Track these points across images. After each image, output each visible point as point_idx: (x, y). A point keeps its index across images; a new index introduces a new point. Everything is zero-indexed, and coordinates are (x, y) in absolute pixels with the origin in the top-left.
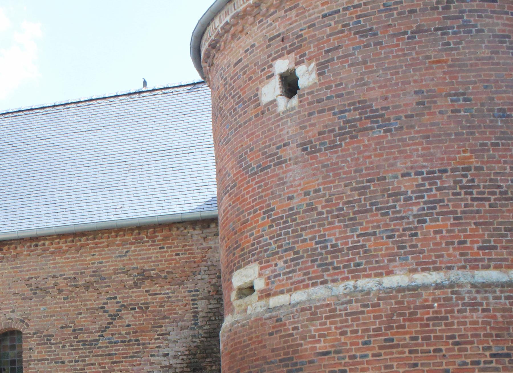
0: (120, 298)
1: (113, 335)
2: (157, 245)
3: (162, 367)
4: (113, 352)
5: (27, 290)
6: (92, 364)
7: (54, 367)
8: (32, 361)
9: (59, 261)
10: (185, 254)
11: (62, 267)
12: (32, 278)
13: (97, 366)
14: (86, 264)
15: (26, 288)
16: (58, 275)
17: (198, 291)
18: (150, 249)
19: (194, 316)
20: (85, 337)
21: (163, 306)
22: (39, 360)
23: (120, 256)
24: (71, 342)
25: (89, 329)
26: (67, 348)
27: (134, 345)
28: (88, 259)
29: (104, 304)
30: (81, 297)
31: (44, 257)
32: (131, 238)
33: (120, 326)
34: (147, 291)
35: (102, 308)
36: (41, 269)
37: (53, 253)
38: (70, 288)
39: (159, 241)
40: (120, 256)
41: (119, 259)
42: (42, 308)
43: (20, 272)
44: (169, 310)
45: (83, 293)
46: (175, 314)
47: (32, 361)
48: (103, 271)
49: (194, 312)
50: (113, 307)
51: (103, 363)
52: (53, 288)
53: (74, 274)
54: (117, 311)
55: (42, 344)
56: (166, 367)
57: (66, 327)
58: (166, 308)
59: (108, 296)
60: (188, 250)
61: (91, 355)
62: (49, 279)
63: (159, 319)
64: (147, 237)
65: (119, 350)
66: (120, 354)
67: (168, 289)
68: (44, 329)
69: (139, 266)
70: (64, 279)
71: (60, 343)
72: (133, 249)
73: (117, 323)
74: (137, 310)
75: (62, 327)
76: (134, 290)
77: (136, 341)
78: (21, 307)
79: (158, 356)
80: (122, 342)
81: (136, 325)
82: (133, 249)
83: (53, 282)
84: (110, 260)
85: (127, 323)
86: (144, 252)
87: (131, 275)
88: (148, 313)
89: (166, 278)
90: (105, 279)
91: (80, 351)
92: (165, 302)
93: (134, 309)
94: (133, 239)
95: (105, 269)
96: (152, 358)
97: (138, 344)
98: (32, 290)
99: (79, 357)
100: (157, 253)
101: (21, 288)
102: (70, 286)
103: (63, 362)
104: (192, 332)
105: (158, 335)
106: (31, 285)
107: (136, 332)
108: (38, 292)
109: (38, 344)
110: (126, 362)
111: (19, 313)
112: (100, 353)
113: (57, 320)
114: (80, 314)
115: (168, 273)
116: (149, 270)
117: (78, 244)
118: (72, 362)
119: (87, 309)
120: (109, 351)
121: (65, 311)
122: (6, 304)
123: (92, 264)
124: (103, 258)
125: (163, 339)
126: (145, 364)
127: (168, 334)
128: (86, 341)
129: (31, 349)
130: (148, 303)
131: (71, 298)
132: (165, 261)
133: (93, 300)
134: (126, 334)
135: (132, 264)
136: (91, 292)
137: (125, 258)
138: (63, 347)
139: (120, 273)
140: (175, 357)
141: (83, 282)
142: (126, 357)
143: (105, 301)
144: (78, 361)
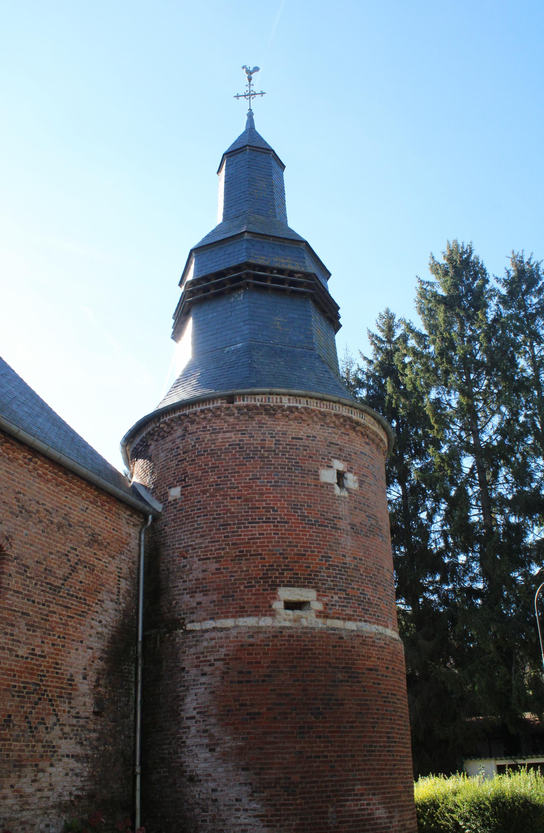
16: (41, 502)
20: (51, 580)
21: (102, 573)
52: (35, 514)
53: (52, 508)
67: (107, 559)
68: (24, 556)
76: (88, 548)
85: (81, 579)
103: (33, 602)
108: (23, 511)
111: (6, 528)
112: (61, 602)
128: (52, 585)
138: (36, 584)
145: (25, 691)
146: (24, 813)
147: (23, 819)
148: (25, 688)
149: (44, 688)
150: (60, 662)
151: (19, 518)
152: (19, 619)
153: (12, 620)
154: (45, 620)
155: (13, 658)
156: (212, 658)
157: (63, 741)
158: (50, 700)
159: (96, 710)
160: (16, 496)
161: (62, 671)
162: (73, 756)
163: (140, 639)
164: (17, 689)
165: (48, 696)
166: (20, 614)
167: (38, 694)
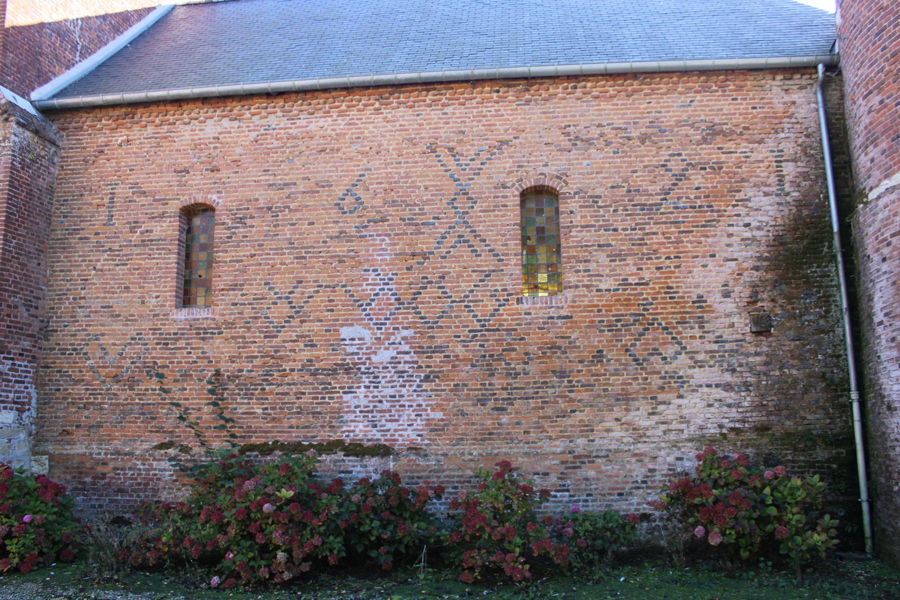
0: (686, 155)
1: (679, 198)
2: (729, 96)
3: (743, 240)
4: (681, 219)
5: (565, 141)
6: (654, 233)
7: (604, 235)
8: (574, 227)
9: (606, 107)
10: (763, 108)
11: (609, 114)
12: (569, 126)
13: (660, 236)
14: (640, 113)
15: (562, 137)
16: (604, 123)
17: (782, 151)
18: (720, 100)
19: (779, 180)
21: (740, 167)
22: (582, 227)
23: (684, 106)
24: (625, 206)
25: (647, 190)
26: (620, 212)
27: (707, 211)
28: (642, 106)
29: (666, 161)
30: (635, 152)
31: (584, 102)
32: (697, 85)
33: (687, 188)
34: (719, 148)
35: (663, 166)
36: (580, 116)
37: (597, 97)
38: (621, 141)
39: (730, 91)
40: (684, 106)
41: (682, 109)
42: (585, 163)
43: (555, 117)
44: (748, 172)
45: (639, 146)
46: (756, 176)
47: (574, 227)
48: (663, 122)
49: (778, 176)
50: (678, 165)
51: (667, 233)
52: (597, 139)
53: (625, 123)
54: (683, 170)
55: (587, 207)
56: (748, 239)
57: (618, 187)
58: (744, 169)
59: (671, 152)
60: (767, 104)
61: (652, 222)
62: (593, 128)
63: (736, 182)
64: (716, 86)
65: (687, 217)
66: (689, 222)
67: (745, 147)
68: (589, 188)
69: (707, 119)
70: (613, 129)
71: (610, 206)
72: (699, 98)
73: (684, 184)
74: (708, 170)
75: (612, 187)
76: (704, 146)
77: (709, 206)
78: (556, 160)
79: (737, 225)
80: (691, 207)
81: (708, 188)
82: (699, 98)
83: (599, 132)
84: (671, 109)
85: (697, 185)
86: (713, 103)
87: (698, 129)
88: (722, 175)
89: (741, 134)
90: (665, 131)
91: (638, 217)
92: (742, 162)
93: (705, 169)
94: (699, 86)
95: (665, 120)
96: (731, 228)
97: (712, 211)
98: (570, 140)
99: (637, 224)
100: (729, 104)
101: (556, 136)
102: (620, 138)
103: (615, 230)
104: (777, 199)
105: (737, 201)
106: (568, 134)
107: (708, 196)
108: (578, 142)
109: (581, 207)
110: (697, 232)
111: (554, 168)
112: (664, 220)
113: (605, 178)
114: (636, 171)
115: (745, 128)
116: (720, 124)
117: (630, 88)
118: (626, 229)
119: (645, 167)
120: (675, 217)
121: (615, 167)
122: (536, 156)
123: (648, 113)
124: (662, 107)
125: (742, 205)
126: (721, 236)
127: (748, 200)
128: (645, 205)
129: (572, 212)
130: (722, 163)
131: (623, 152)
132: (740, 114)
133: (650, 156)
134: (696, 198)
135: (699, 116)
136: (648, 146)
137: (690, 109)
138: (615, 211)
139: (684, 125)
140: (759, 228)
141: (638, 134)
142: (697, 226)
143: (668, 158)
144: (635, 229)
145: (619, 324)
146: (639, 445)
147: (637, 452)
148: (618, 321)
149: (651, 317)
150: (674, 285)
151: (574, 151)
152: (594, 253)
153: (583, 256)
154: (639, 244)
155: (594, 293)
156: (887, 235)
157: (697, 369)
158: (664, 329)
159: (754, 329)
160: (564, 131)
161: (680, 295)
162: (717, 386)
163: (835, 228)
164: (605, 323)
165: (660, 324)
166: (596, 248)
167: (641, 324)
